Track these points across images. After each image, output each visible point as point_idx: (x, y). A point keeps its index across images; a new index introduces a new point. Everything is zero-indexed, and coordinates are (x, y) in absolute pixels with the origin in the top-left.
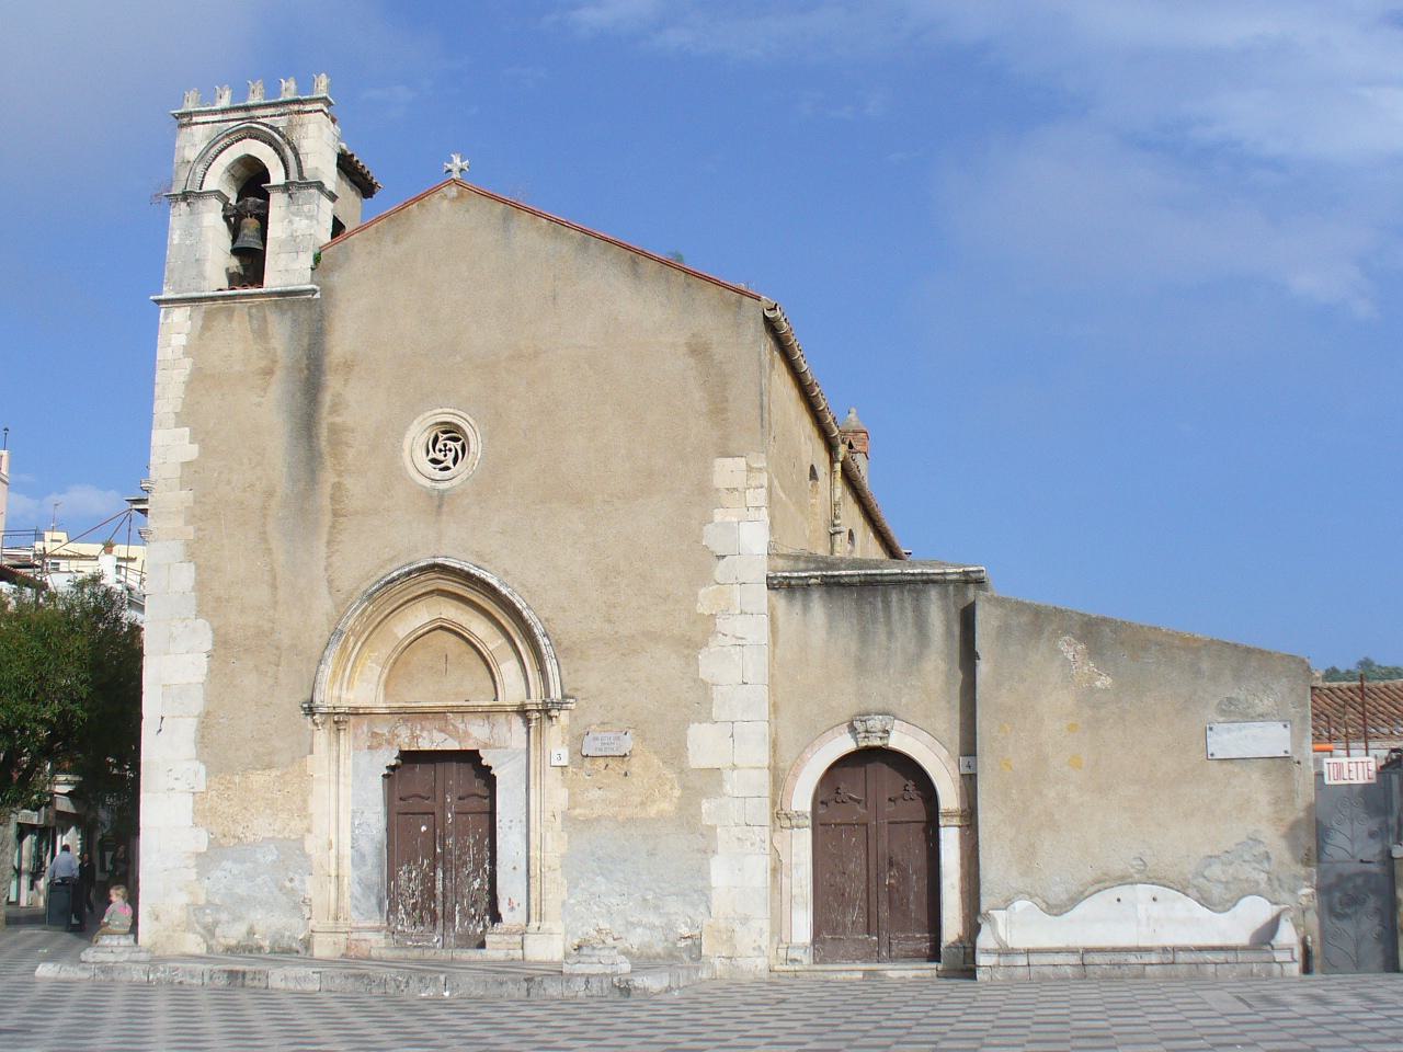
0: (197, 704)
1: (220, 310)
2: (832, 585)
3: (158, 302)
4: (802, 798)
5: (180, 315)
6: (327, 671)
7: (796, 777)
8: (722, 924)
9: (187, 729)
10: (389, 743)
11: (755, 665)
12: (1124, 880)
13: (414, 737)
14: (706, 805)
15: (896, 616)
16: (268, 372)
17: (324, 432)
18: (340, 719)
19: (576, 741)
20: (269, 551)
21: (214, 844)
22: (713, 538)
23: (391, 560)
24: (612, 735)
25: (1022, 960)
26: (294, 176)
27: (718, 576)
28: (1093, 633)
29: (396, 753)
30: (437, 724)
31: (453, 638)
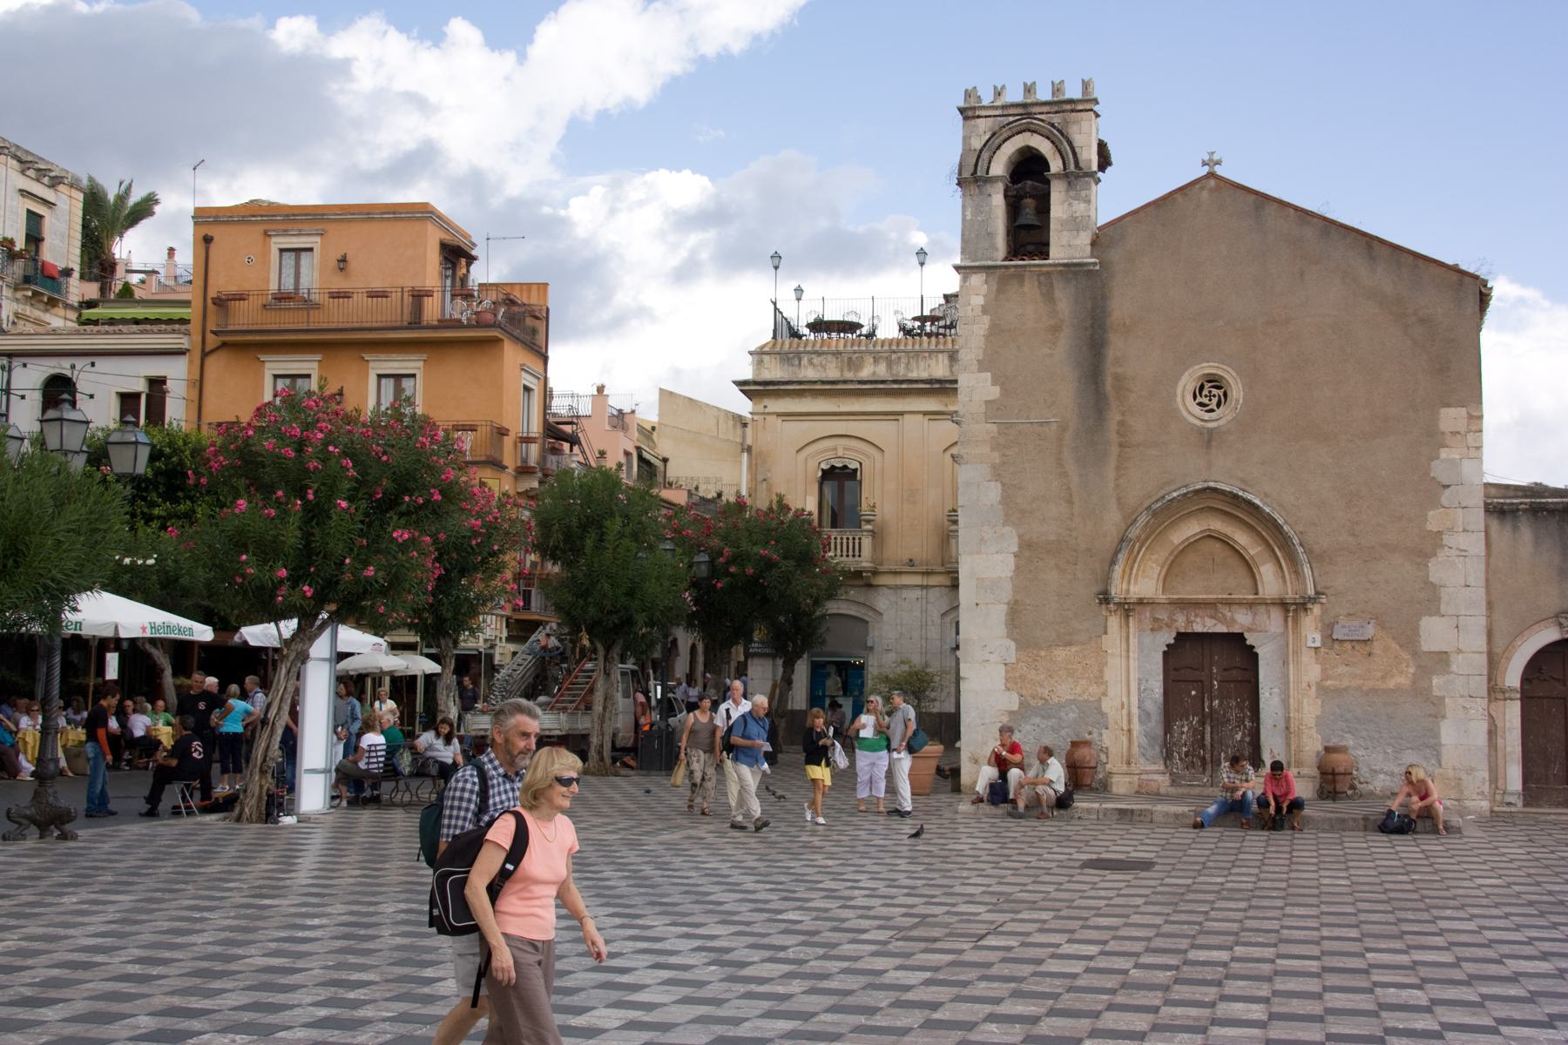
0: (1007, 593)
1: (1013, 276)
2: (1536, 511)
4: (1513, 677)
6: (1118, 570)
7: (1509, 659)
8: (1451, 773)
9: (999, 612)
11: (1475, 572)
13: (1189, 622)
14: (1435, 681)
16: (1055, 329)
17: (1109, 382)
18: (1127, 609)
20: (1065, 474)
21: (1023, 704)
22: (1439, 471)
23: (1169, 483)
24: (1356, 623)
26: (1072, 167)
27: (1444, 501)
29: (1174, 634)
31: (1218, 545)
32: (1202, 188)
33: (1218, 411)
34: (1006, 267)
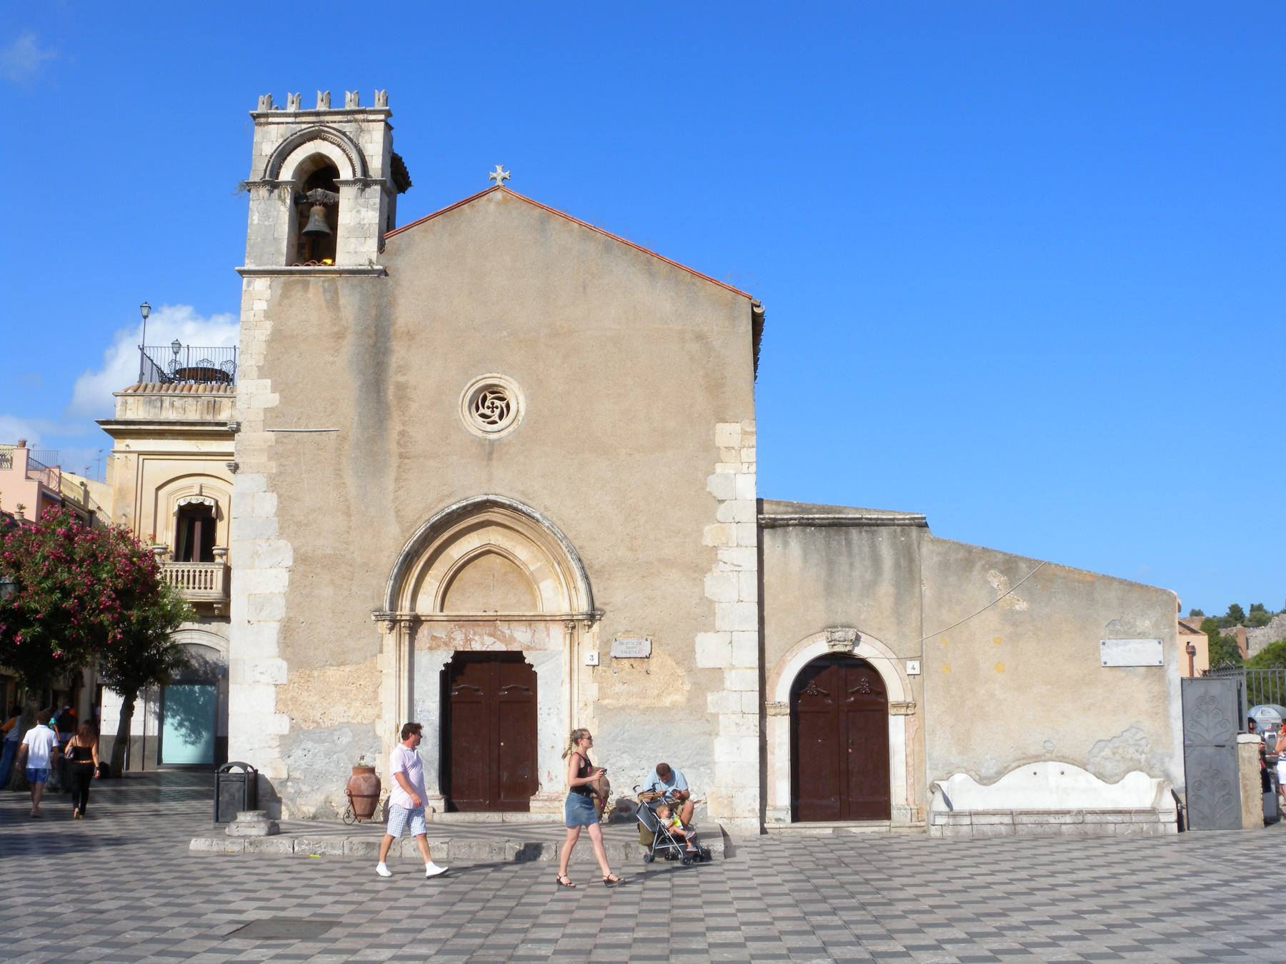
0: (280, 612)
1: (299, 282)
2: (805, 524)
3: (242, 273)
4: (781, 692)
5: (261, 284)
7: (779, 674)
9: (271, 630)
10: (446, 644)
12: (1037, 758)
13: (468, 640)
14: (711, 698)
15: (856, 550)
16: (339, 336)
19: (606, 644)
22: (715, 485)
24: (635, 640)
25: (967, 820)
26: (359, 175)
27: (719, 516)
28: (1009, 565)
30: (487, 630)
32: (489, 200)
33: (502, 424)
34: (291, 272)
